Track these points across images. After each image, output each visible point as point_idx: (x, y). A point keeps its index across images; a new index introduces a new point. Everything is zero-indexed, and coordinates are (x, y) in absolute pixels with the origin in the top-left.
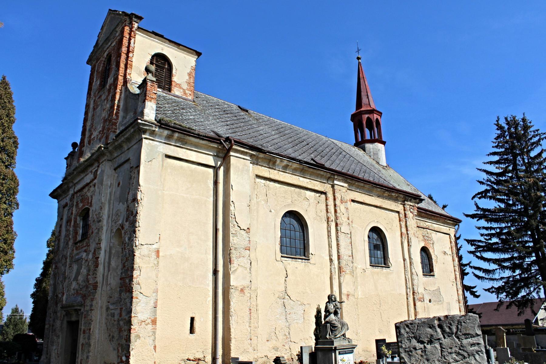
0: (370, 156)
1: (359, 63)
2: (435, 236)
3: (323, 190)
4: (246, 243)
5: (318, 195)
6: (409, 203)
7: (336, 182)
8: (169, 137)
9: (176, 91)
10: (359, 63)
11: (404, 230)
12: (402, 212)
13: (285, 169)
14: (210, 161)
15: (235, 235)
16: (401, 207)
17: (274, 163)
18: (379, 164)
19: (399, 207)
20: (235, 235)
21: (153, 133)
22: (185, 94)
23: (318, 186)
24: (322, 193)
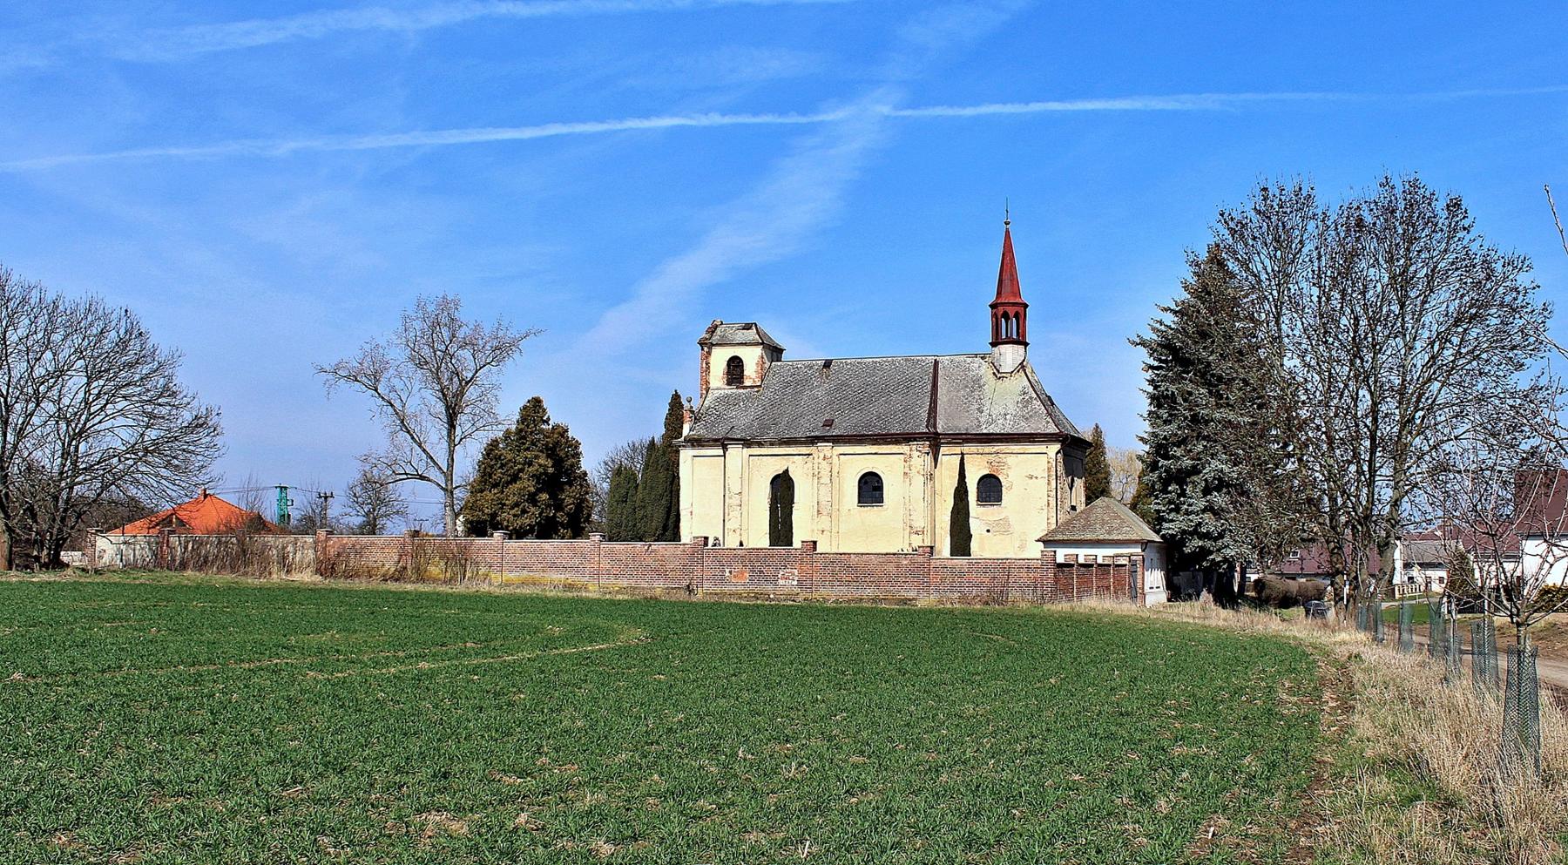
0: (993, 364)
1: (1007, 229)
2: (1011, 460)
3: (808, 452)
4: (739, 502)
5: (805, 457)
6: (915, 443)
7: (819, 444)
8: (693, 446)
9: (747, 383)
10: (1007, 229)
11: (907, 470)
12: (908, 453)
13: (772, 444)
14: (721, 452)
15: (730, 498)
16: (908, 448)
17: (763, 445)
18: (998, 371)
19: (904, 448)
20: (730, 498)
21: (683, 446)
22: (754, 381)
23: (804, 450)
24: (809, 455)
